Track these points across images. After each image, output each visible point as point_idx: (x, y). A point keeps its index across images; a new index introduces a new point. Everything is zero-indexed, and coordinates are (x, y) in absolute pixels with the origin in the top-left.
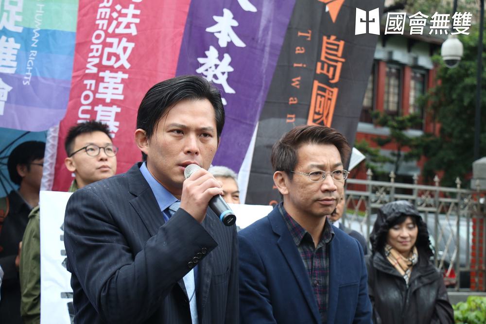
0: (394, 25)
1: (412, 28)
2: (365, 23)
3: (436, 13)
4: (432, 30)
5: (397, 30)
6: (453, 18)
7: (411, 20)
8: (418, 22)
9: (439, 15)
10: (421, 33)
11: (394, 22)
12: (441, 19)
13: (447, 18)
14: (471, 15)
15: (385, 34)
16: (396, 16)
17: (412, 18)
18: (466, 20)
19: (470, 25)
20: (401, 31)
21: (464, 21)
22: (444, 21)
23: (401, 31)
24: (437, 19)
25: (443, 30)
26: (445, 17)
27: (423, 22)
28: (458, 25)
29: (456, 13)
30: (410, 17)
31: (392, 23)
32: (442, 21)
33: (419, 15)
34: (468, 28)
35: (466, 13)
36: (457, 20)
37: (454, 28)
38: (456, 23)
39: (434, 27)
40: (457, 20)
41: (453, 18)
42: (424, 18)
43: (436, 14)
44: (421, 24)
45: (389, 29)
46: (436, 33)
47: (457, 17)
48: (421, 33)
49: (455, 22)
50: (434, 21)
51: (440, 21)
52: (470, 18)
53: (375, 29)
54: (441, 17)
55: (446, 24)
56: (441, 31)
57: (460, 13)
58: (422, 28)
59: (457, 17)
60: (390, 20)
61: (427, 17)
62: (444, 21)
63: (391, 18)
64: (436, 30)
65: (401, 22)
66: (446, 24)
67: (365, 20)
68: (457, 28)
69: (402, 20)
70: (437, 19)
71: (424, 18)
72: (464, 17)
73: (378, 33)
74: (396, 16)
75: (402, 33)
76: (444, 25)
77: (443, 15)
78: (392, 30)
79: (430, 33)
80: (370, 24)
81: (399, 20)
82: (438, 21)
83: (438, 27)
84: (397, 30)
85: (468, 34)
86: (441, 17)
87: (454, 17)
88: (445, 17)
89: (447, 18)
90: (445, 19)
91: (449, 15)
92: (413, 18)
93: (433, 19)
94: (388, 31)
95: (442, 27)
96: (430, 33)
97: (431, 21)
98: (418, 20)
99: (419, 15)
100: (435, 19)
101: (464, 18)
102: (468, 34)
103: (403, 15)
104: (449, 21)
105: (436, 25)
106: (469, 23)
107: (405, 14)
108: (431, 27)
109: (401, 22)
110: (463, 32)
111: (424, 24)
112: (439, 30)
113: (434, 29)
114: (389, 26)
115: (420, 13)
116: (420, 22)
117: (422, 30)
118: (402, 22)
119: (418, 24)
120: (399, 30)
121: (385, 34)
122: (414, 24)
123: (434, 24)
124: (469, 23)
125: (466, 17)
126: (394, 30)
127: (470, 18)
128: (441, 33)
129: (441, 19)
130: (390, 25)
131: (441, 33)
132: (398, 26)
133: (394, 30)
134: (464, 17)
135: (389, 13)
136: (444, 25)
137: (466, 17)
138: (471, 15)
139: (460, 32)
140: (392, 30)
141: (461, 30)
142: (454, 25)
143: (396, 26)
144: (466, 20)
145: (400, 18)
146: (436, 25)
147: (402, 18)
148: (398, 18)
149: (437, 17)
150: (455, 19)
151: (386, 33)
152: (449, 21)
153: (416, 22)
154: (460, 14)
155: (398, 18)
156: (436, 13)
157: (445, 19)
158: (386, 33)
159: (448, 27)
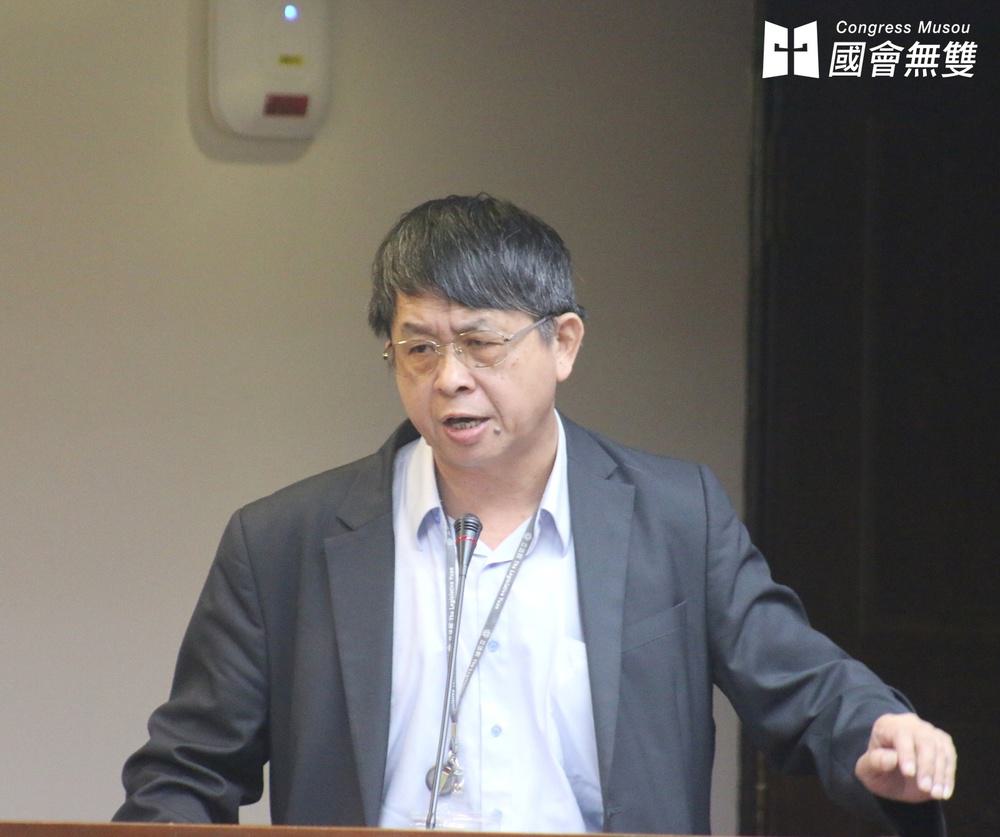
0: (845, 61)
1: (875, 66)
2: (786, 53)
3: (917, 43)
4: (909, 71)
5: (850, 70)
6: (945, 50)
7: (874, 55)
8: (885, 57)
9: (922, 47)
10: (891, 75)
11: (845, 57)
12: (924, 53)
13: (934, 51)
14: (976, 46)
15: (830, 75)
16: (848, 48)
17: (878, 51)
18: (967, 54)
19: (974, 62)
20: (857, 71)
21: (964, 56)
22: (930, 56)
23: (857, 71)
24: (918, 53)
25: (929, 70)
26: (931, 50)
27: (895, 57)
28: (953, 61)
29: (951, 43)
30: (872, 50)
31: (842, 59)
32: (927, 56)
33: (887, 46)
34: (971, 66)
35: (966, 43)
36: (951, 54)
37: (947, 66)
38: (951, 59)
39: (913, 65)
40: (951, 54)
41: (945, 50)
42: (895, 51)
43: (916, 45)
44: (891, 60)
45: (837, 67)
46: (917, 74)
47: (952, 49)
48: (891, 75)
49: (948, 56)
50: (913, 56)
51: (924, 56)
52: (974, 56)
53: (807, 66)
54: (925, 50)
55: (933, 61)
56: (925, 71)
57: (957, 43)
58: (893, 66)
59: (952, 49)
60: (837, 54)
61: (901, 49)
62: (930, 56)
63: (839, 51)
64: (917, 71)
65: (857, 57)
66: (933, 61)
67: (786, 47)
68: (952, 67)
69: (859, 54)
70: (918, 53)
71: (895, 51)
72: (963, 49)
73: (816, 75)
74: (848, 48)
75: (859, 74)
76: (929, 62)
77: (928, 47)
78: (842, 70)
79: (907, 75)
80: (796, 53)
81: (854, 55)
82: (920, 56)
83: (919, 65)
84: (850, 70)
85: (970, 75)
86: (925, 50)
87: (947, 49)
88: (931, 50)
89: (934, 51)
90: (931, 52)
91: (938, 46)
92: (878, 51)
93: (912, 53)
94: (835, 71)
95: (926, 65)
96: (907, 75)
97: (908, 56)
98: (885, 55)
99: (887, 46)
100: (915, 52)
101: (965, 51)
102: (970, 75)
103: (860, 47)
104: (938, 56)
105: (916, 62)
106: (972, 59)
107: (863, 44)
108: (907, 65)
109: (857, 57)
110: (962, 73)
111: (897, 61)
112: (921, 70)
113: (913, 69)
114: (836, 64)
115: (889, 43)
116: (888, 57)
117: (892, 70)
118: (859, 59)
119: (885, 60)
120: (854, 69)
121: (830, 75)
122: (880, 60)
123: (913, 61)
124: (972, 59)
125: (968, 49)
126: (846, 70)
127: (974, 56)
128: (925, 74)
129: (924, 53)
130: (839, 61)
131: (925, 74)
132: (852, 63)
133: (846, 70)
134: (963, 49)
135: (836, 44)
136: (929, 62)
137: (968, 49)
138: (976, 46)
139: (956, 73)
140: (842, 70)
141: (959, 70)
142: (947, 61)
143: (848, 64)
144: (967, 54)
145: (855, 51)
146: (916, 62)
147: (858, 51)
148: (851, 51)
149: (918, 50)
150: (949, 52)
151: (832, 74)
152: (938, 56)
153: (882, 57)
154: (957, 45)
155: (851, 51)
156: (917, 43)
157: (931, 52)
158: (832, 74)
159: (936, 66)
